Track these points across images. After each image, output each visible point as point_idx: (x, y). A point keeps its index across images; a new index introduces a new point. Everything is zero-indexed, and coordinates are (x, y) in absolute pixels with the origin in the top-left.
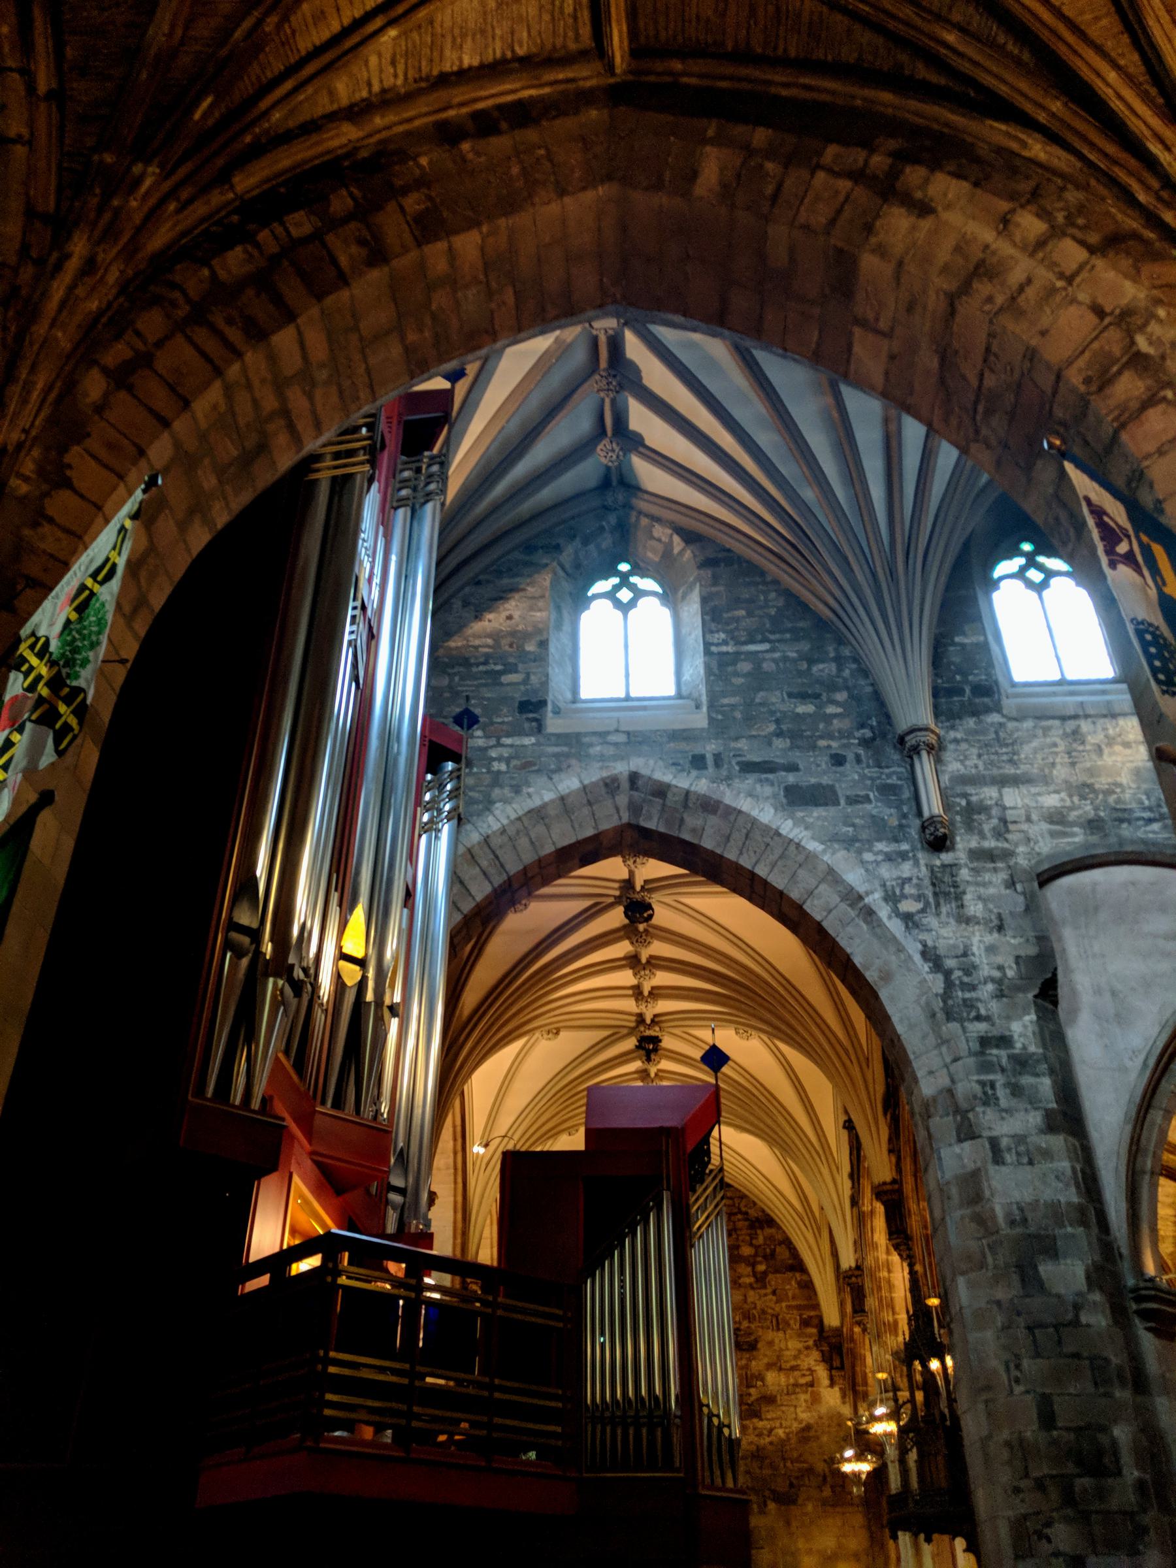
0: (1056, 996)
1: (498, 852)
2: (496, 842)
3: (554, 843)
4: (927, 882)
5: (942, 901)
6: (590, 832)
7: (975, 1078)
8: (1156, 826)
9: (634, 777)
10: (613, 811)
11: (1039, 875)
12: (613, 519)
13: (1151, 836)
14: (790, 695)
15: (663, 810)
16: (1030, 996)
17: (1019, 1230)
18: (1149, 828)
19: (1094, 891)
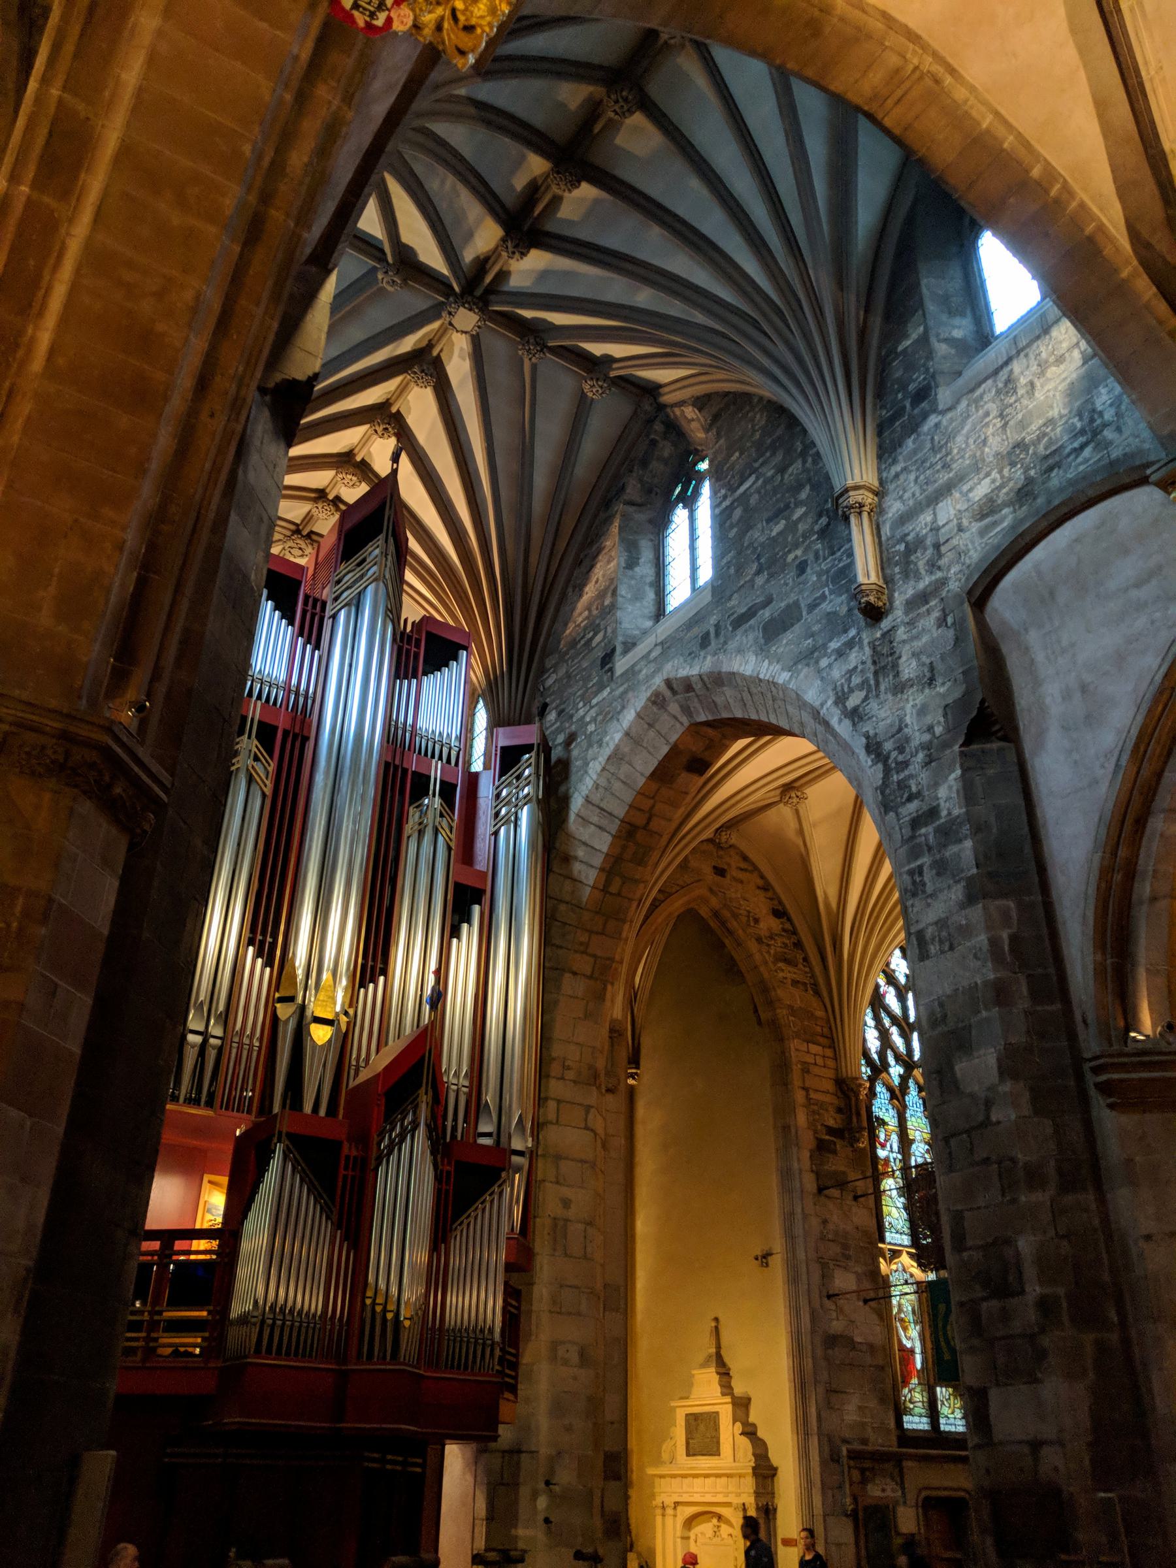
0: (1016, 729)
1: (601, 805)
2: (596, 798)
3: (642, 774)
4: (869, 662)
5: (881, 679)
6: (665, 749)
7: (907, 868)
8: (1087, 452)
9: (668, 683)
10: (673, 722)
11: (970, 593)
12: (658, 427)
13: (1081, 468)
14: (769, 520)
15: (700, 701)
16: (956, 748)
17: (940, 1029)
18: (1080, 459)
19: (1039, 573)
